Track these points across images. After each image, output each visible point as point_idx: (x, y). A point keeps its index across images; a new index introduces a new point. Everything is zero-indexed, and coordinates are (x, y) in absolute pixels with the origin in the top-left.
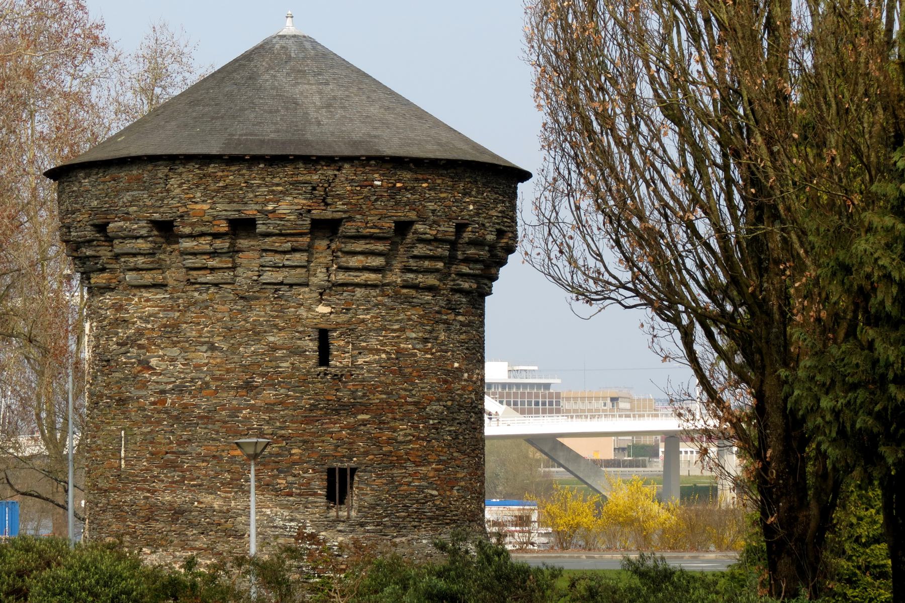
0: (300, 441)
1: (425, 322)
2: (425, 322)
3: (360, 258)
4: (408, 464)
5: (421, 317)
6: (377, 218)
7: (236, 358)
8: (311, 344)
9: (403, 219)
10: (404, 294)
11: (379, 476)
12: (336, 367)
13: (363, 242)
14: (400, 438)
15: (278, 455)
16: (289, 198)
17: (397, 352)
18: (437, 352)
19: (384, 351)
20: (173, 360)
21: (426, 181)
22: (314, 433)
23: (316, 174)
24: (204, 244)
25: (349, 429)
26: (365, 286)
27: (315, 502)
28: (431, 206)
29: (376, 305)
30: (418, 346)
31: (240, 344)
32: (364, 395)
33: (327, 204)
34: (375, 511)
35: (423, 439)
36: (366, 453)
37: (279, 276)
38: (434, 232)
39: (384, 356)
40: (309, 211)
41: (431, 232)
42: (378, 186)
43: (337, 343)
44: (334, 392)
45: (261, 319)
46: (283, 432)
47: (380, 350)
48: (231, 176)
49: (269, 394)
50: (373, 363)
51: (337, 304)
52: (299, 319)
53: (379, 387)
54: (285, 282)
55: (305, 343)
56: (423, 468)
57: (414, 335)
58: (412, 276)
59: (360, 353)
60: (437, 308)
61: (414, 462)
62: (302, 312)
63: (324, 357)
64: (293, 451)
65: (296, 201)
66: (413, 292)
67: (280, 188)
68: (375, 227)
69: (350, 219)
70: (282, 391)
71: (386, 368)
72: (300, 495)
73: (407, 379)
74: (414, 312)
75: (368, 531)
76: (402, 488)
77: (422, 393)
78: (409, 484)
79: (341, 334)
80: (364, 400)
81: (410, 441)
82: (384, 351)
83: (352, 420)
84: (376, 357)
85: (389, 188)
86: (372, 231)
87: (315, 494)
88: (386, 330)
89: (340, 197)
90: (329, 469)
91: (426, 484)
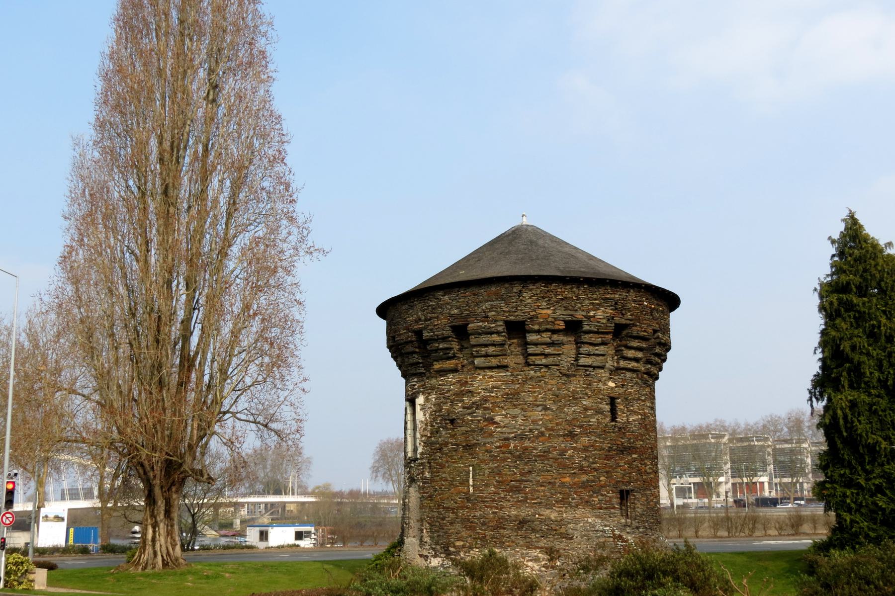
3: (633, 351)
7: (563, 415)
20: (514, 417)
24: (546, 337)
31: (565, 406)
33: (623, 314)
40: (613, 318)
48: (566, 292)
49: (585, 440)
52: (599, 390)
62: (601, 385)
64: (602, 478)
68: (645, 331)
70: (593, 438)
72: (606, 508)
83: (629, 458)
87: (614, 508)
89: (629, 310)
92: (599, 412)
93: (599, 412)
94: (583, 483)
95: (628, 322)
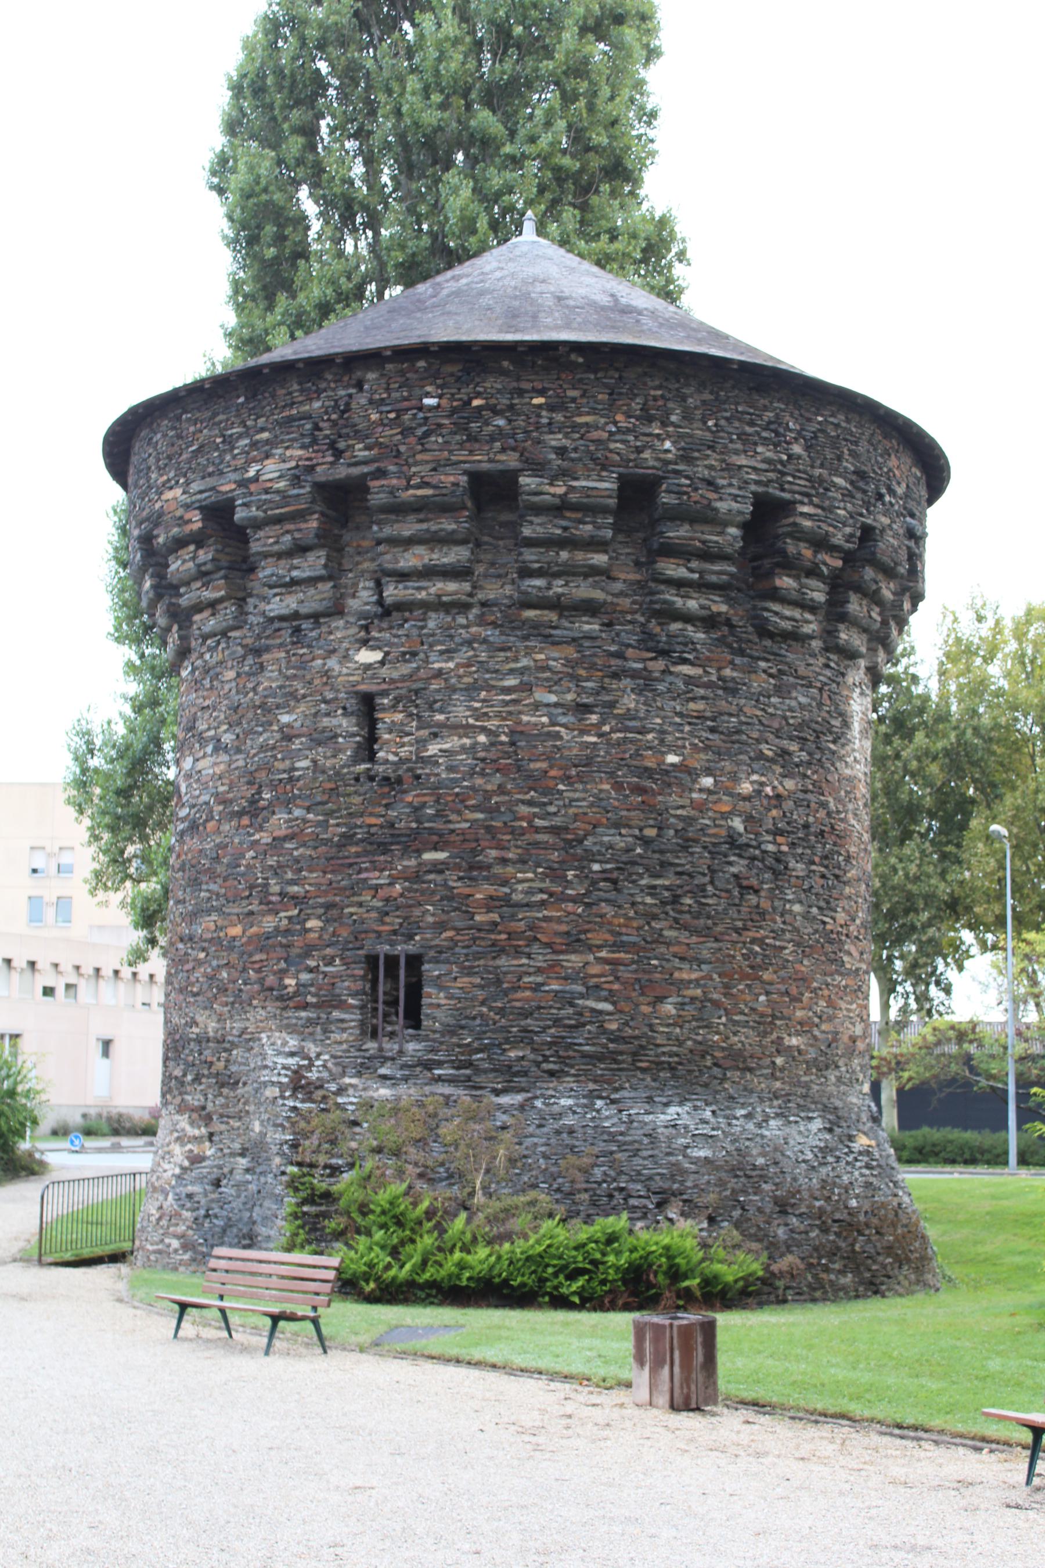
0: (322, 906)
1: (583, 673)
2: (583, 673)
3: (420, 550)
4: (535, 948)
5: (568, 662)
6: (429, 467)
8: (345, 723)
9: (486, 466)
10: (528, 620)
11: (469, 972)
13: (412, 518)
14: (517, 897)
15: (287, 932)
16: (279, 451)
17: (512, 733)
18: (612, 731)
19: (484, 730)
21: (542, 392)
22: (345, 889)
23: (318, 398)
25: (406, 879)
26: (440, 605)
27: (342, 1021)
28: (556, 440)
29: (469, 643)
30: (563, 720)
32: (439, 814)
34: (455, 1040)
35: (574, 900)
36: (440, 926)
37: (290, 603)
38: (560, 490)
39: (482, 738)
41: (552, 490)
42: (431, 408)
43: (388, 718)
44: (381, 810)
45: (274, 685)
46: (296, 888)
47: (473, 726)
50: (458, 753)
51: (390, 644)
53: (469, 798)
54: (304, 610)
55: (335, 722)
56: (573, 957)
57: (553, 698)
58: (539, 582)
59: (435, 735)
60: (613, 648)
61: (548, 945)
62: (332, 663)
64: (309, 924)
65: (288, 453)
66: (553, 616)
67: (265, 435)
69: (381, 473)
70: (298, 812)
71: (485, 765)
73: (535, 781)
74: (556, 655)
75: (439, 1079)
76: (519, 995)
77: (571, 811)
78: (536, 988)
79: (397, 700)
80: (438, 825)
81: (543, 903)
82: (484, 730)
83: (413, 862)
84: (467, 741)
85: (454, 411)
86: (420, 492)
87: (342, 1005)
88: (489, 688)
89: (359, 435)
91: (580, 989)
92: (325, 738)
93: (325, 738)
95: (356, 471)
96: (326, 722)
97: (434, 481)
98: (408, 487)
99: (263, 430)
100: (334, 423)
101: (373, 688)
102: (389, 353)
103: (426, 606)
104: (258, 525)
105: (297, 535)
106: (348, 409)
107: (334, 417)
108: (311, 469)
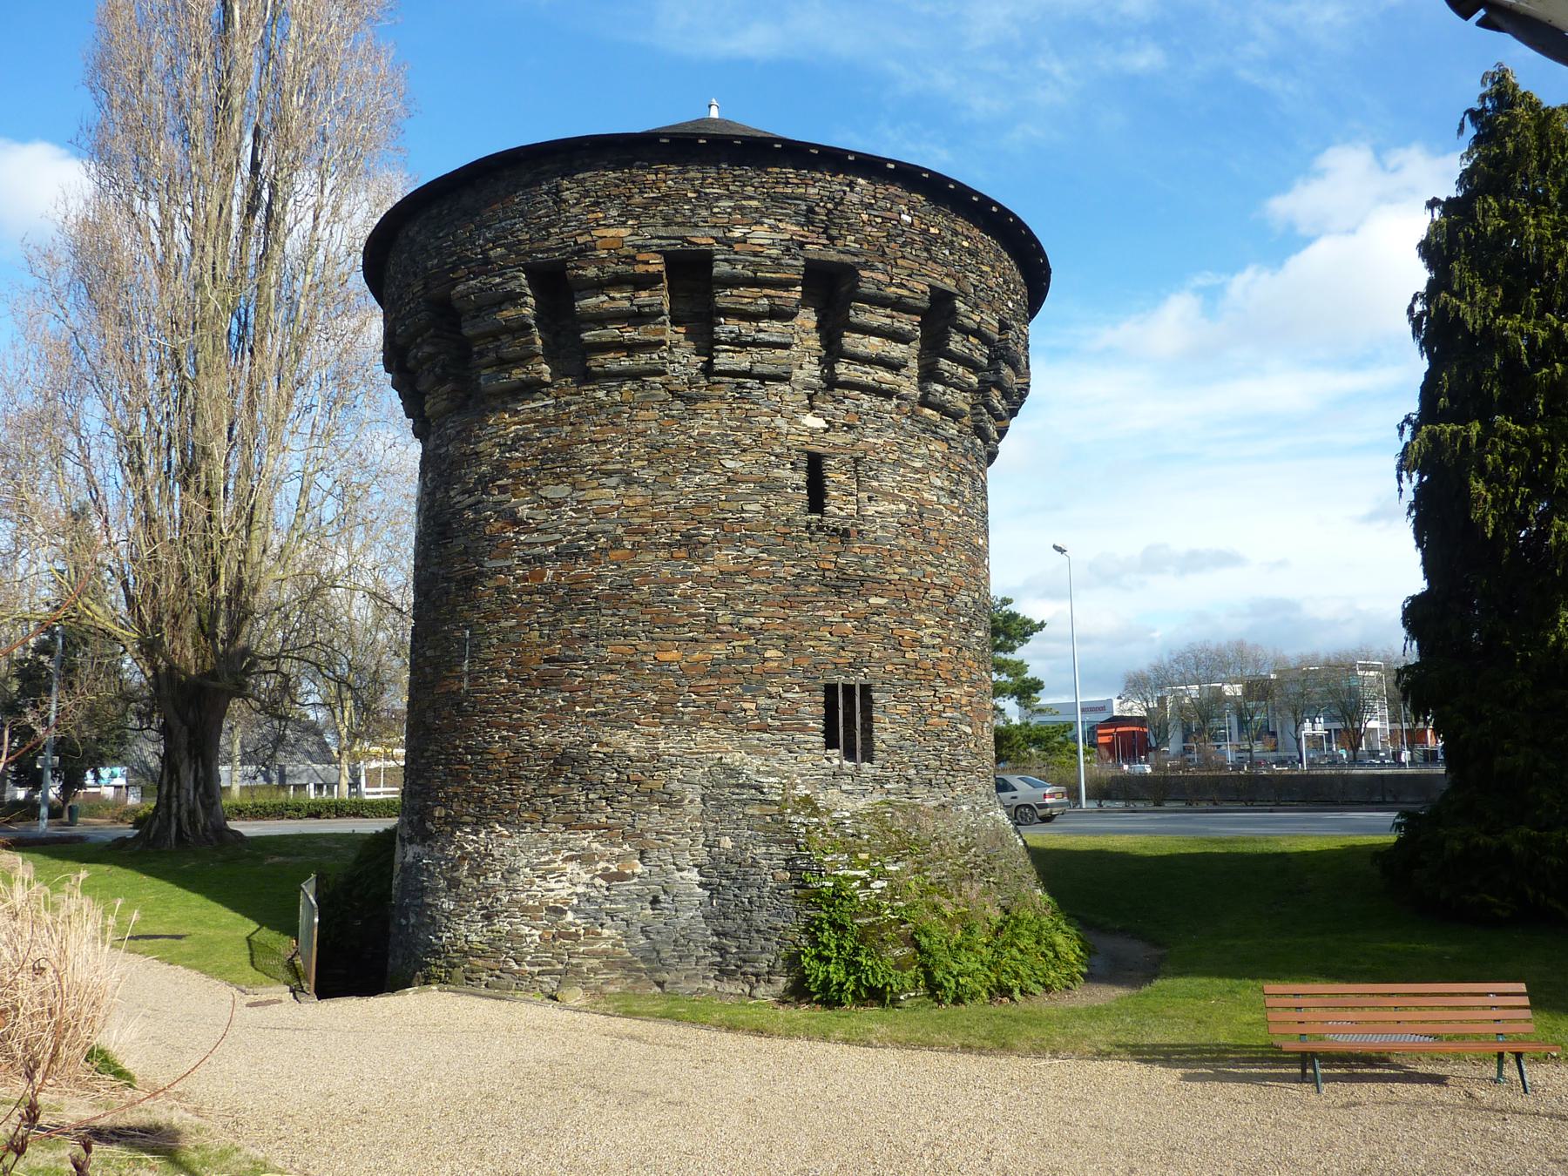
3: (875, 340)
7: (669, 496)
12: (835, 515)
14: (927, 640)
20: (556, 505)
24: (620, 300)
25: (857, 619)
30: (944, 500)
31: (676, 472)
33: (831, 238)
39: (903, 507)
40: (802, 245)
43: (836, 477)
46: (750, 620)
48: (666, 179)
49: (725, 558)
52: (776, 434)
62: (779, 421)
63: (817, 500)
67: (754, 203)
68: (901, 286)
70: (748, 551)
83: (860, 605)
86: (900, 291)
87: (804, 729)
90: (826, 686)
92: (769, 486)
94: (716, 663)
95: (847, 259)
96: (777, 472)
97: (910, 285)
98: (891, 284)
99: (751, 198)
100: (830, 211)
101: (820, 450)
102: (891, 166)
103: (865, 389)
104: (734, 282)
105: (777, 302)
106: (841, 203)
107: (830, 206)
108: (802, 245)
